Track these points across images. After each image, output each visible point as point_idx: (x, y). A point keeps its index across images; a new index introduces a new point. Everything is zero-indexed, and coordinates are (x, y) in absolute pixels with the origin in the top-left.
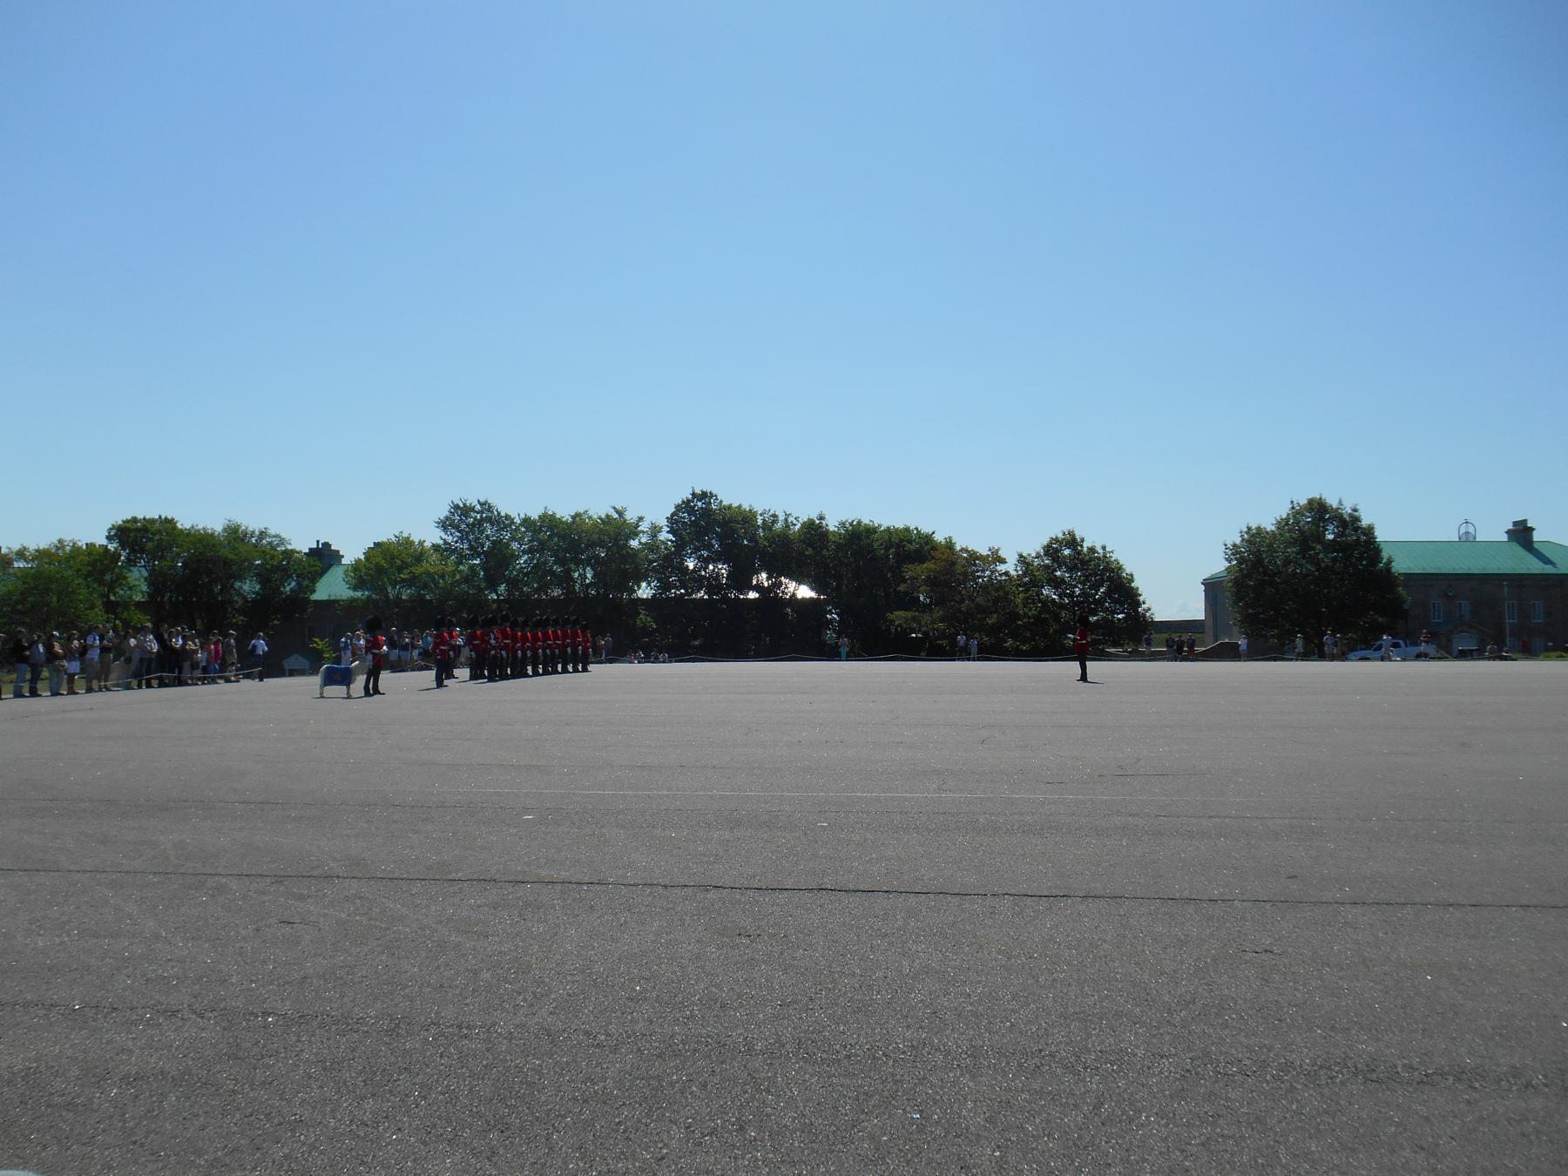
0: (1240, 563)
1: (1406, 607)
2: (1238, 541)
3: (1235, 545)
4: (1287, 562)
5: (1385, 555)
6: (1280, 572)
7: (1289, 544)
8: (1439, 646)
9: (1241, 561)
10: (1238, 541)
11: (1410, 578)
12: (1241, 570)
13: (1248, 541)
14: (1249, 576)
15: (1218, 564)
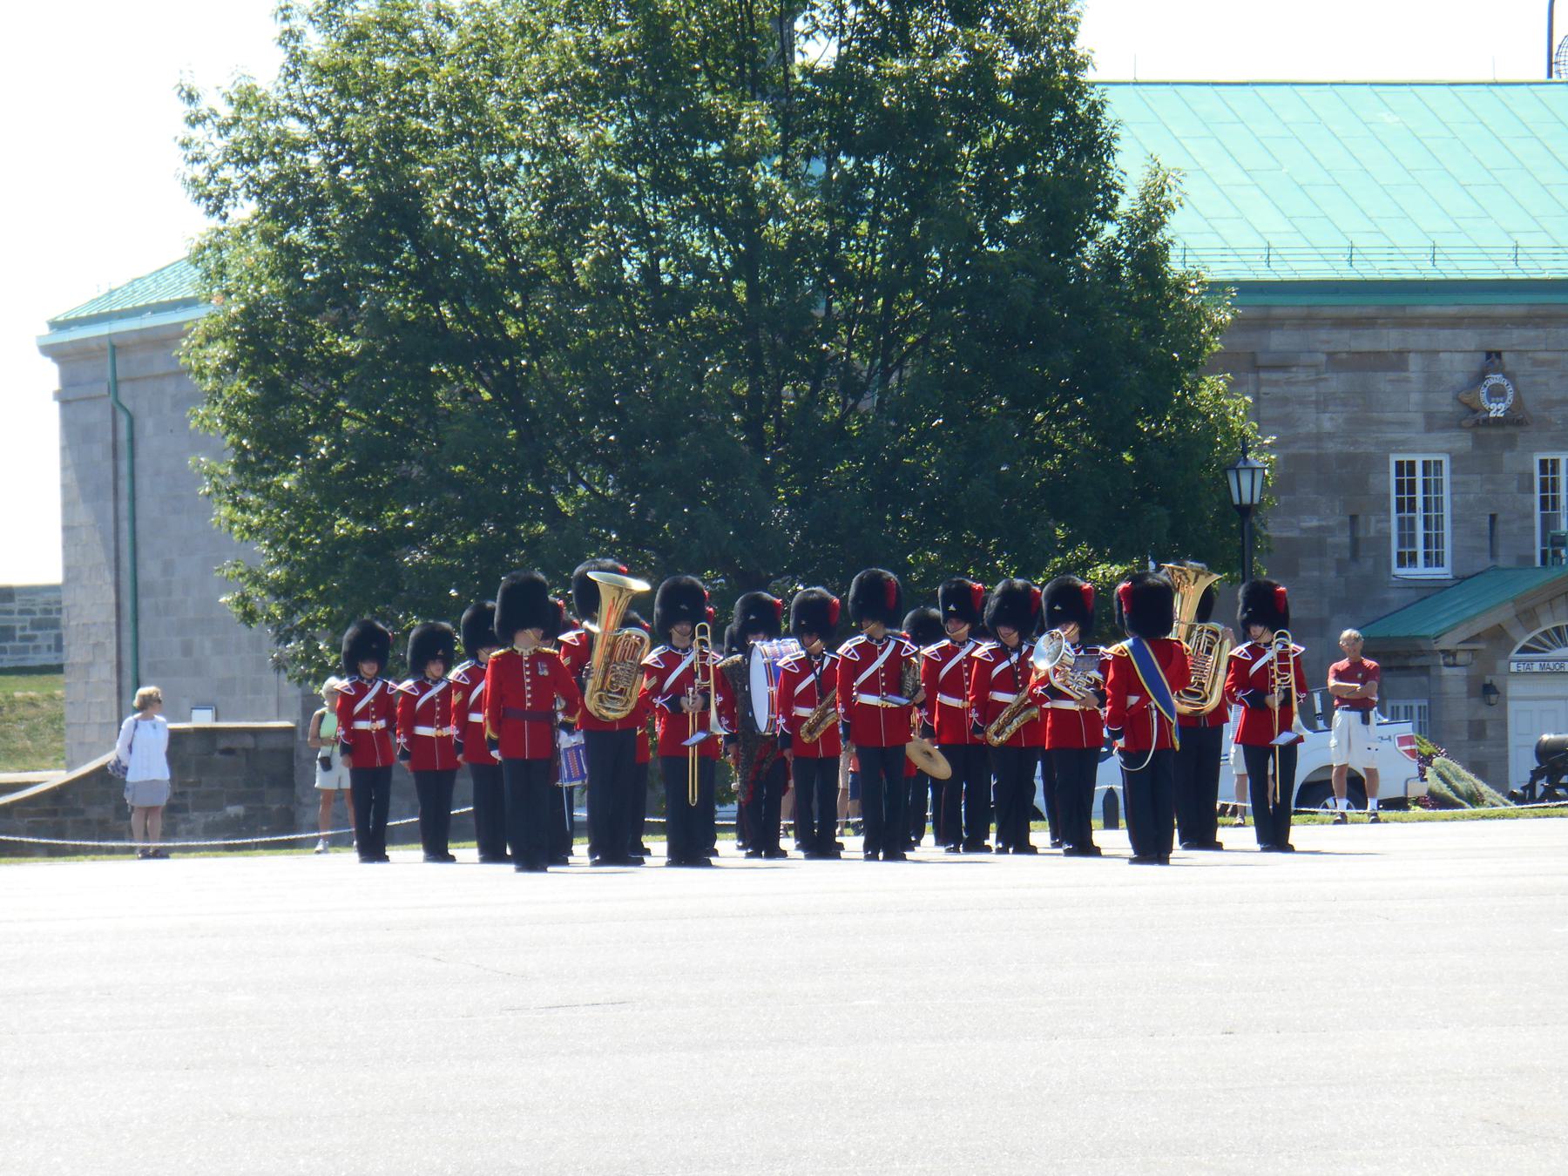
0: (285, 215)
1: (1245, 489)
2: (266, 71)
3: (246, 100)
4: (567, 208)
5: (1129, 169)
6: (531, 284)
7: (585, 92)
8: (1434, 729)
9: (289, 201)
10: (266, 71)
11: (1267, 303)
12: (289, 261)
13: (337, 75)
14: (335, 295)
15: (146, 228)
